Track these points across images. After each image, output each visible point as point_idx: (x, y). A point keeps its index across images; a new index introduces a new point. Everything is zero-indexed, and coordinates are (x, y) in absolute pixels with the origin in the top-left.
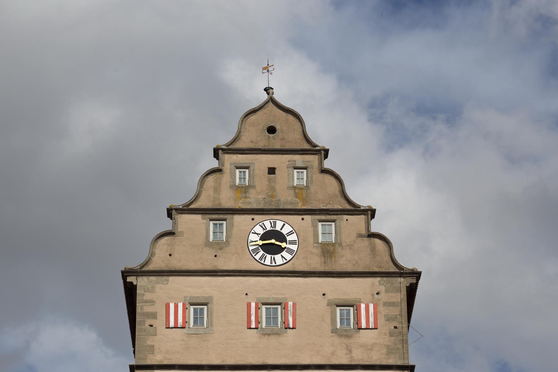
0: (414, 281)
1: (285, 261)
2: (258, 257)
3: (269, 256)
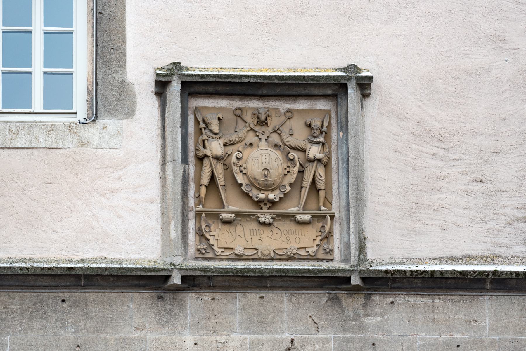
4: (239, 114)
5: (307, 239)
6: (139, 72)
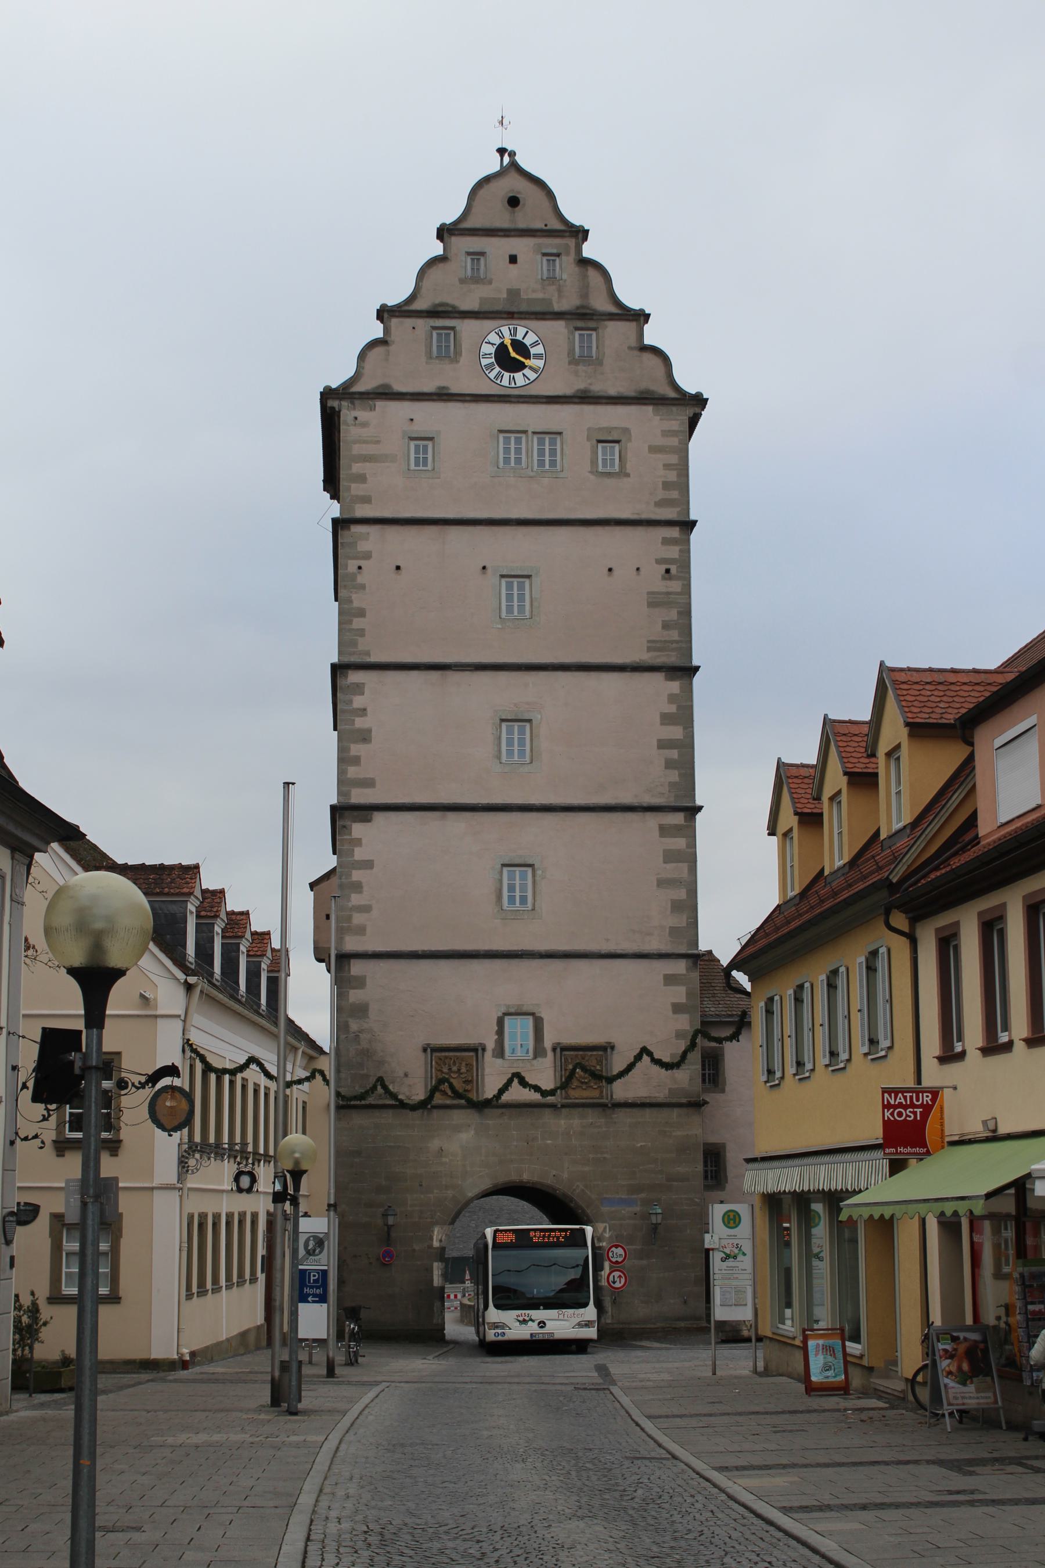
0: (697, 410)
1: (528, 382)
2: (492, 375)
3: (506, 375)
4: (576, 1056)
5: (596, 1094)
6: (548, 1044)
